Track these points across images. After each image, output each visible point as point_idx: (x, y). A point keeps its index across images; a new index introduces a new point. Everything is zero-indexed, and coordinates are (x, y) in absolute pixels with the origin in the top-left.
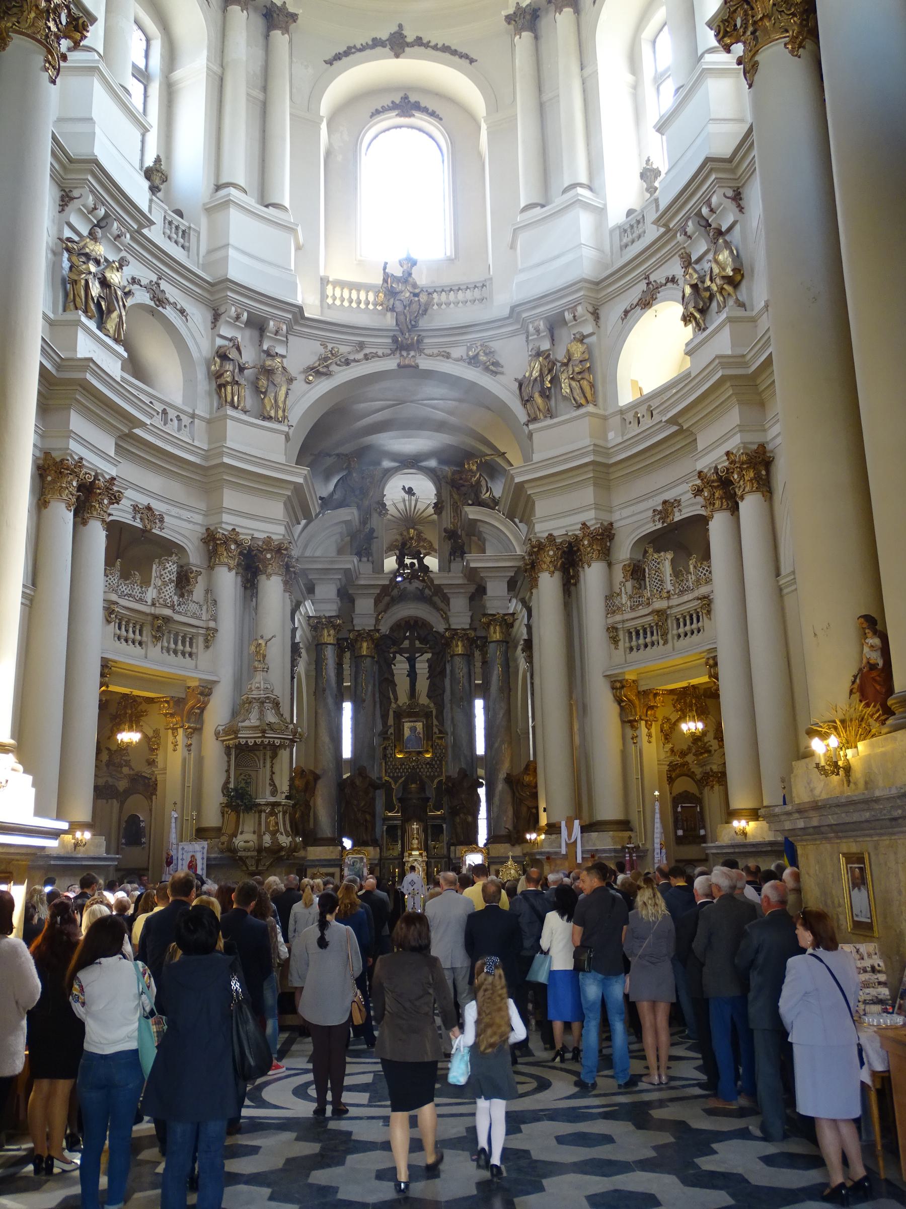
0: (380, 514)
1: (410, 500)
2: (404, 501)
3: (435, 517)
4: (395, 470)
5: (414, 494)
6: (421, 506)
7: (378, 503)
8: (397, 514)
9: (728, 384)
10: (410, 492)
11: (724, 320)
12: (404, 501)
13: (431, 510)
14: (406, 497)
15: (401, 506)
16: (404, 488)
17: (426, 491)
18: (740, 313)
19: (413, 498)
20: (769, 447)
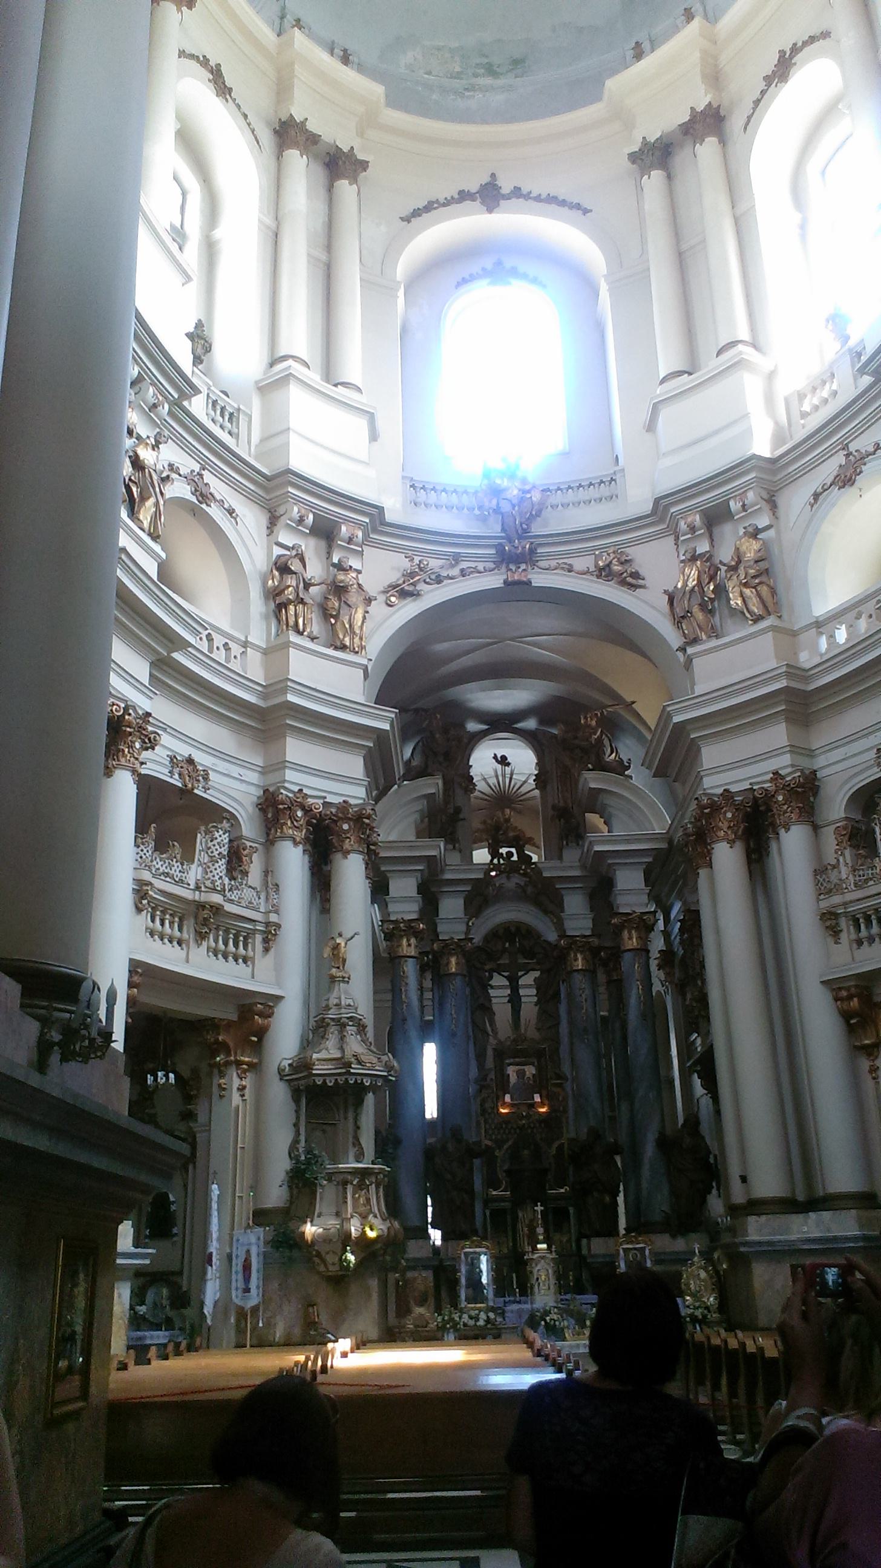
1: (504, 776)
2: (496, 771)
3: (537, 792)
5: (508, 764)
6: (518, 778)
8: (487, 790)
9: (783, 697)
10: (503, 761)
11: (768, 627)
12: (496, 771)
16: (495, 757)
17: (524, 760)
18: (777, 623)
19: (508, 769)
20: (819, 775)
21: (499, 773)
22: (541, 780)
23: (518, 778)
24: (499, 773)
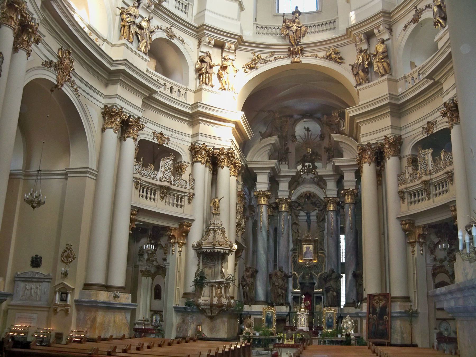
0: (293, 141)
1: (308, 135)
2: (305, 134)
4: (301, 119)
7: (292, 136)
8: (301, 141)
10: (308, 129)
12: (305, 134)
14: (306, 132)
15: (304, 138)
16: (305, 128)
19: (310, 133)
21: (306, 134)
24: (306, 134)
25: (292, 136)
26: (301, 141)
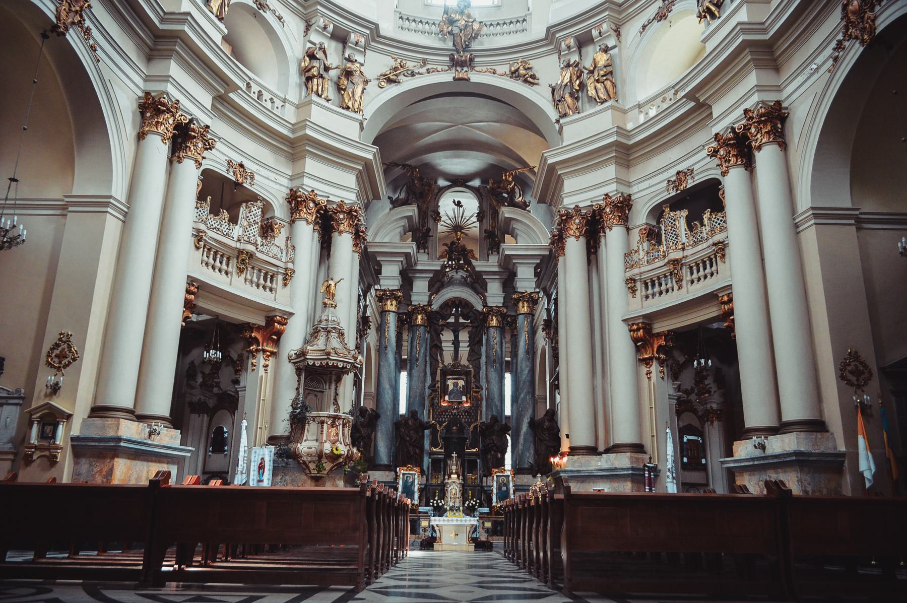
3: (478, 224)
4: (449, 187)
7: (434, 211)
8: (449, 222)
10: (459, 204)
13: (474, 219)
15: (451, 215)
16: (454, 202)
17: (471, 204)
19: (461, 209)
22: (480, 216)
23: (467, 214)
25: (434, 211)
26: (449, 222)
